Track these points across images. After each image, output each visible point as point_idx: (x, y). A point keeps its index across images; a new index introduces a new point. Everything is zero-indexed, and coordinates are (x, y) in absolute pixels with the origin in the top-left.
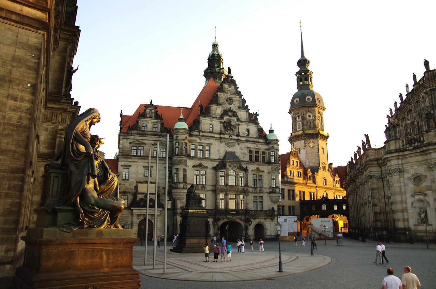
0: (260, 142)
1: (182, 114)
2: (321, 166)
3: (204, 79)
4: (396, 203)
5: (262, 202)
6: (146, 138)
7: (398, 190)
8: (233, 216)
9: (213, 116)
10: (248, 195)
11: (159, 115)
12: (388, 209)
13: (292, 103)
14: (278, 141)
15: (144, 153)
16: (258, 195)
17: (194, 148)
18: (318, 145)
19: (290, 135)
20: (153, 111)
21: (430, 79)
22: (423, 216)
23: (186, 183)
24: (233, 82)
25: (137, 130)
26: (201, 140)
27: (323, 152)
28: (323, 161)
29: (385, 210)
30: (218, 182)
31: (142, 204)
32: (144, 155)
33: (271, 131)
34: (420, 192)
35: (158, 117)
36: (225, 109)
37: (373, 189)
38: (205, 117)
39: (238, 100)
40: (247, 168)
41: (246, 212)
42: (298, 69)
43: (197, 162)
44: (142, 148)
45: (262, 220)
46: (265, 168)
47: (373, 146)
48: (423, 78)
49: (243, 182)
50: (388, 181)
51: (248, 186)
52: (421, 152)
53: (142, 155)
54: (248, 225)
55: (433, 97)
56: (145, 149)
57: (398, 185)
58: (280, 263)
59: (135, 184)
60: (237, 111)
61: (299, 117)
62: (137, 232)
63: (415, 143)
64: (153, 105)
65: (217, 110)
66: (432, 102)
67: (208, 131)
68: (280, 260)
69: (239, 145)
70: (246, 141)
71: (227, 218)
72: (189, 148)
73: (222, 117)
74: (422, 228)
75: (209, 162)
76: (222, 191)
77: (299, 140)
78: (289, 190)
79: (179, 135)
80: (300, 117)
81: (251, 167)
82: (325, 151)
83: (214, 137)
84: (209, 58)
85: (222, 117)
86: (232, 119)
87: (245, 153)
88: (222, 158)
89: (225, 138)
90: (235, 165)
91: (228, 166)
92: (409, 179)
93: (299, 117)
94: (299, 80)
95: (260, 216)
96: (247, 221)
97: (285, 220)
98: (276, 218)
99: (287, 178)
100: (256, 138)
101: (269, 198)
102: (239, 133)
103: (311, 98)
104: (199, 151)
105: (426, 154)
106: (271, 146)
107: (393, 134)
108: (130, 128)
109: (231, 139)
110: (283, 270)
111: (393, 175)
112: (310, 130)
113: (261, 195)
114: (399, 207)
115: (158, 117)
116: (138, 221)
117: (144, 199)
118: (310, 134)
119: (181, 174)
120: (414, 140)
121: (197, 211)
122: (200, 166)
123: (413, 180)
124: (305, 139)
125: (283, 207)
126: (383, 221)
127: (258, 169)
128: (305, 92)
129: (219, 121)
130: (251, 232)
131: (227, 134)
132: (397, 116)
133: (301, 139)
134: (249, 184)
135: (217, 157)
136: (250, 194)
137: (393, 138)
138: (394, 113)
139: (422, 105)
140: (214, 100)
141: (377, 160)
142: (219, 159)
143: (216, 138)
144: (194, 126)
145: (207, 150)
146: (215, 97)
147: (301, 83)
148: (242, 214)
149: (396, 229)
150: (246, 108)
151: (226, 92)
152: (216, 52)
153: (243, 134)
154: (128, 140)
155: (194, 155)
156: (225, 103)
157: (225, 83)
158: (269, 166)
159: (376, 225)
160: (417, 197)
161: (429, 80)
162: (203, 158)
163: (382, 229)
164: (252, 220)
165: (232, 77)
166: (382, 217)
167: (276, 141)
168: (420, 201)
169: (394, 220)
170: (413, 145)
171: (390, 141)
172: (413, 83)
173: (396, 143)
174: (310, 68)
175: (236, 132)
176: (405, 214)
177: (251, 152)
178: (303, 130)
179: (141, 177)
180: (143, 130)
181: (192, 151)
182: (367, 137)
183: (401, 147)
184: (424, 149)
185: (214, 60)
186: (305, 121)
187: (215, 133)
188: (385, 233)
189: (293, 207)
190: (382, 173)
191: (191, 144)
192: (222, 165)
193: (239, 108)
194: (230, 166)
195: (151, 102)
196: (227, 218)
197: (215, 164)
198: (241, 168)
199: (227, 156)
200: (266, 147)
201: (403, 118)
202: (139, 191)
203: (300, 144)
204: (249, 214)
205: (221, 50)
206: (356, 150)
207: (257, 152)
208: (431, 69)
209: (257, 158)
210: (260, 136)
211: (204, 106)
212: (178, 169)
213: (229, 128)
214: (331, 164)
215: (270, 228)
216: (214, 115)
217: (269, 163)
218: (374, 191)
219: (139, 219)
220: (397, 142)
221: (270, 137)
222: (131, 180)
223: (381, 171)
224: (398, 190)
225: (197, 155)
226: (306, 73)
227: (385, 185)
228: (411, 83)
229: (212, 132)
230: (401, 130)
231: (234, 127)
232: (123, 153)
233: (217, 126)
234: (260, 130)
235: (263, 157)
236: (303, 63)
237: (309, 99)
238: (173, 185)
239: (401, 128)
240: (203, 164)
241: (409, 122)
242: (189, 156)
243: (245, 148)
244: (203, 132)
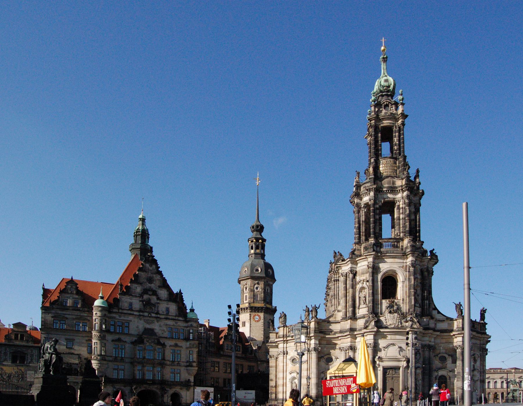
0: (179, 320)
43: (116, 337)
61: (246, 288)
70: (164, 318)
80: (248, 289)
83: (133, 314)
88: (141, 333)
89: (144, 316)
93: (246, 288)
100: (175, 316)
102: (158, 311)
103: (260, 270)
106: (190, 323)
118: (255, 307)
122: (119, 340)
131: (146, 312)
143: (136, 315)
145: (126, 327)
147: (252, 251)
153: (163, 312)
162: (123, 333)
174: (264, 235)
187: (135, 311)
192: (139, 340)
221: (190, 315)
231: (154, 305)
240: (122, 339)
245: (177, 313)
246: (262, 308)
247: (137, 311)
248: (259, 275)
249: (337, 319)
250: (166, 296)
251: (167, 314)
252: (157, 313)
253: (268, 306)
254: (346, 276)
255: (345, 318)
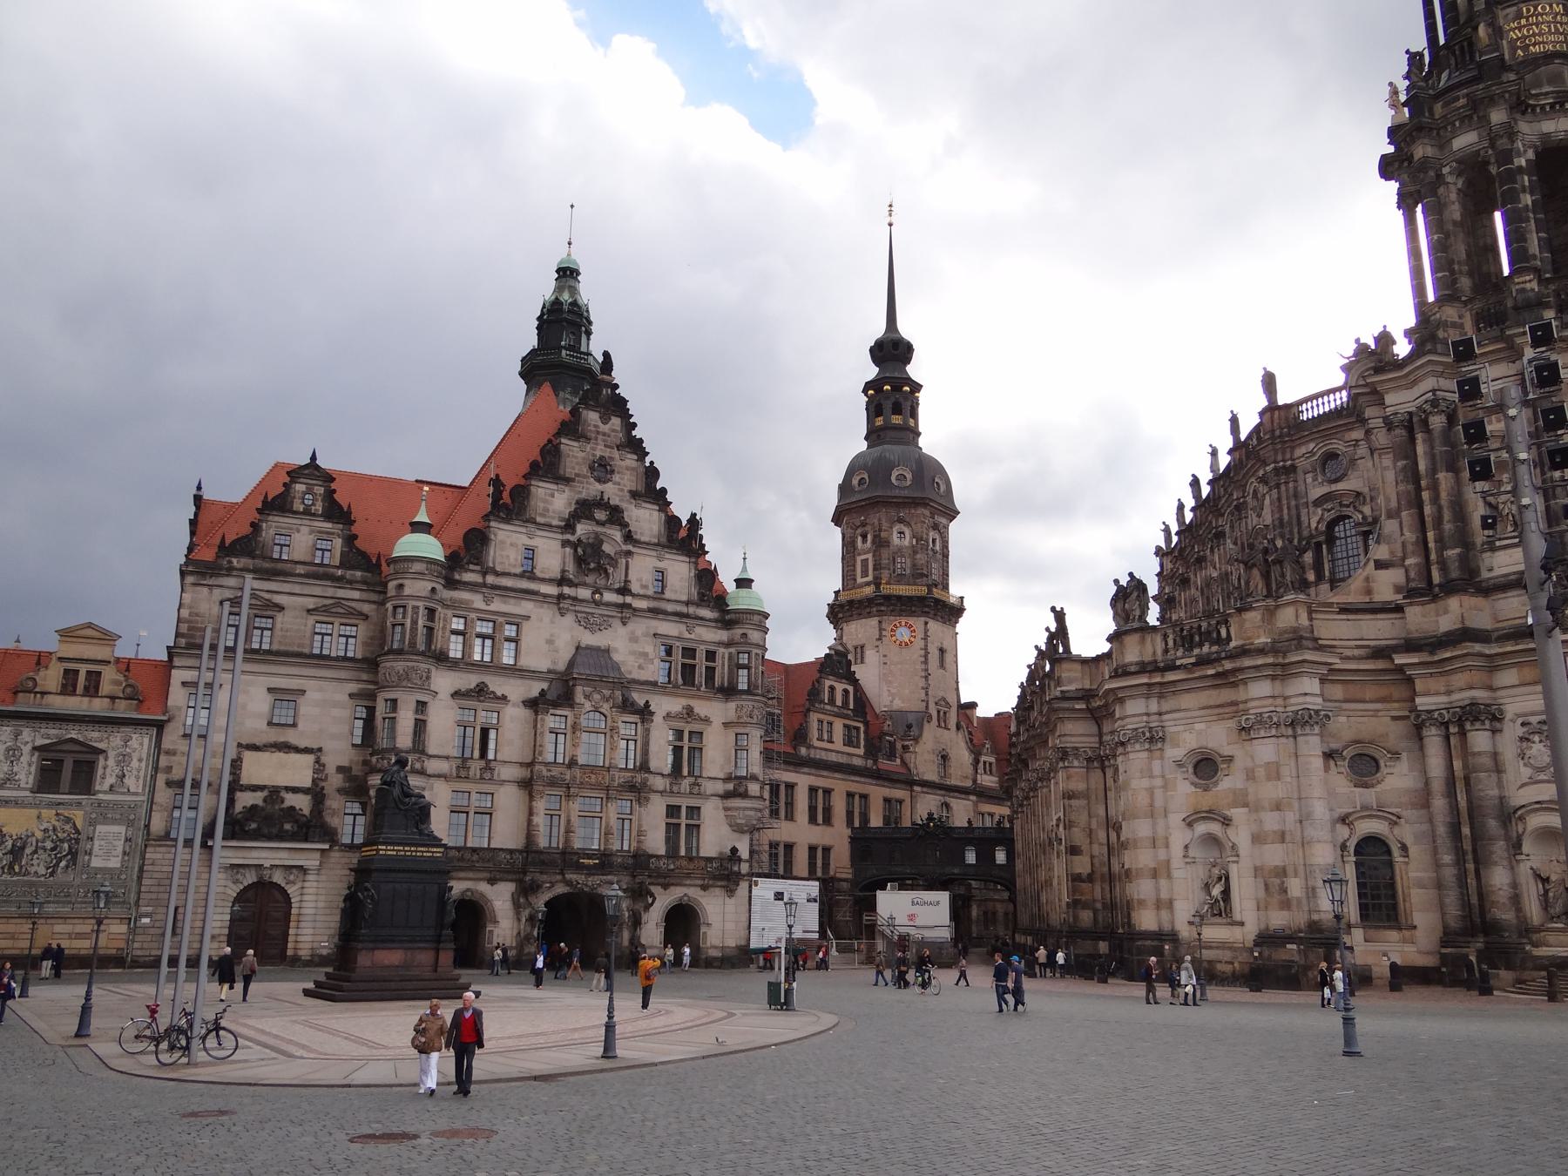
0: (702, 619)
1: (423, 508)
2: (933, 711)
3: (522, 386)
4: (1136, 847)
5: (698, 826)
6: (286, 587)
7: (1142, 800)
8: (590, 875)
9: (539, 519)
10: (647, 799)
11: (340, 507)
12: (1116, 868)
13: (844, 488)
14: (766, 616)
15: (275, 640)
16: (685, 803)
17: (461, 627)
18: (925, 638)
19: (831, 598)
20: (322, 490)
21: (1277, 433)
22: (1216, 891)
23: (423, 752)
24: (619, 406)
25: (251, 554)
26: (487, 601)
27: (942, 665)
28: (941, 694)
29: (1106, 869)
30: (541, 753)
31: (254, 826)
32: (275, 647)
33: (744, 583)
34: (1209, 812)
35: (336, 512)
36: (583, 496)
37: (1069, 796)
38: (507, 521)
39: (633, 469)
40: (647, 704)
41: (639, 861)
42: (872, 372)
43: (470, 681)
44: (268, 623)
45: (694, 893)
46: (715, 711)
47: (1075, 650)
48: (1257, 430)
49: (631, 755)
50: (1116, 770)
51: (648, 771)
52: (1218, 675)
53: (265, 647)
54: (639, 906)
55: (1284, 495)
56: (278, 626)
57: (1145, 783)
58: (610, 1028)
59: (232, 753)
60: (624, 505)
61: (864, 537)
62: (226, 931)
63: (1201, 645)
64: (318, 468)
65: (554, 501)
66: (1280, 509)
67: (518, 570)
68: (610, 1017)
69: (624, 624)
70: (650, 610)
71: (568, 883)
72: (444, 628)
73: (569, 526)
74: (1213, 933)
75: (512, 681)
76: (553, 783)
77: (860, 616)
78: (813, 790)
79: (406, 582)
81: (663, 705)
82: (948, 658)
84: (542, 314)
85: (569, 526)
86: (604, 534)
87: (645, 655)
88: (561, 667)
89: (575, 599)
90: (607, 693)
91: (579, 697)
92: (1179, 764)
93: (864, 537)
94: (874, 409)
95: (688, 876)
96: (640, 895)
97: (779, 896)
98: (744, 885)
99: (809, 747)
100: (687, 603)
101: (722, 813)
102: (626, 581)
103: (909, 476)
104: (478, 641)
105: (1234, 685)
106: (738, 632)
107: (1138, 613)
108: (226, 550)
109: (597, 604)
110: (619, 1052)
111: (1129, 749)
112: (899, 582)
113: (693, 802)
114: (1141, 858)
115: (336, 512)
116: (233, 891)
117: (263, 809)
118: (899, 598)
119: (406, 719)
120: (1200, 634)
121: (408, 851)
122: (481, 692)
123: (1191, 770)
124: (880, 613)
125: (789, 847)
126: (1099, 906)
127: (689, 712)
128: (892, 451)
129: (560, 537)
130: (652, 931)
131: (585, 585)
132: (1182, 550)
133: (869, 615)
134: (654, 764)
135: (542, 664)
136: (655, 798)
137: (1136, 625)
138: (1175, 539)
139: (1253, 520)
140: (547, 465)
141: (1087, 695)
142: (549, 672)
143: (545, 596)
144: (469, 550)
145: (508, 640)
146: (549, 452)
147: (879, 421)
148: (624, 867)
149: (1135, 935)
150: (659, 498)
151: (588, 439)
152: (566, 297)
153: (645, 587)
154: (217, 591)
155: (459, 655)
156: (585, 477)
157: (588, 407)
158: (727, 700)
159: (1076, 917)
160: (1202, 828)
161: (1273, 437)
162: (495, 667)
163: (1094, 935)
164: (656, 890)
165: (617, 386)
166: (1098, 895)
167: (756, 618)
168: (1212, 840)
169: (1129, 906)
170: (1196, 651)
171: (1126, 632)
172: (1230, 445)
173: (1143, 641)
174: (914, 370)
175: (617, 578)
176: (1163, 882)
177: (669, 652)
178: (877, 583)
179: (254, 724)
180: (276, 556)
181: (453, 637)
182: (1060, 616)
183: (1159, 657)
184: (1228, 665)
185: (563, 321)
186: (885, 553)
187: (543, 580)
188: (1103, 947)
189: (827, 850)
190: (1101, 743)
191: (449, 613)
192: (558, 693)
193: (634, 495)
194: (587, 697)
195: (314, 457)
196: (568, 883)
197: (535, 688)
198: (627, 706)
199: (579, 660)
200: (723, 635)
201: (1201, 561)
202: (244, 781)
203: (861, 630)
204: (647, 868)
205: (588, 292)
206: (1031, 657)
207: (689, 652)
208: (1280, 403)
209: (688, 671)
210: (702, 596)
211: (510, 482)
212: (395, 701)
213: (592, 565)
214: (973, 705)
215: (720, 919)
216: (542, 515)
217: (729, 692)
218: (1073, 802)
219: (236, 882)
220: (1148, 638)
221: (739, 600)
222: (217, 738)
223: (1100, 735)
224: (1142, 800)
225: (470, 656)
226: (897, 388)
227: (1110, 782)
228: (1225, 443)
229: (529, 575)
230: (1194, 600)
232: (192, 636)
233: (552, 556)
234: (707, 577)
235: (710, 671)
236: (892, 352)
237: (902, 477)
238: (374, 759)
239: (1193, 591)
241: (1215, 574)
242: (441, 658)
243: (646, 635)
244: (497, 574)
245: (694, 592)
246: (921, 599)
247: (550, 581)
248: (906, 493)
249: (1377, 598)
250: (655, 528)
251: (659, 595)
252: (624, 590)
253: (937, 593)
254: (1410, 430)
255: (1422, 590)
